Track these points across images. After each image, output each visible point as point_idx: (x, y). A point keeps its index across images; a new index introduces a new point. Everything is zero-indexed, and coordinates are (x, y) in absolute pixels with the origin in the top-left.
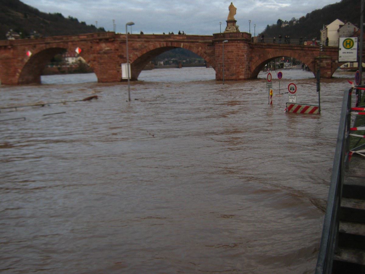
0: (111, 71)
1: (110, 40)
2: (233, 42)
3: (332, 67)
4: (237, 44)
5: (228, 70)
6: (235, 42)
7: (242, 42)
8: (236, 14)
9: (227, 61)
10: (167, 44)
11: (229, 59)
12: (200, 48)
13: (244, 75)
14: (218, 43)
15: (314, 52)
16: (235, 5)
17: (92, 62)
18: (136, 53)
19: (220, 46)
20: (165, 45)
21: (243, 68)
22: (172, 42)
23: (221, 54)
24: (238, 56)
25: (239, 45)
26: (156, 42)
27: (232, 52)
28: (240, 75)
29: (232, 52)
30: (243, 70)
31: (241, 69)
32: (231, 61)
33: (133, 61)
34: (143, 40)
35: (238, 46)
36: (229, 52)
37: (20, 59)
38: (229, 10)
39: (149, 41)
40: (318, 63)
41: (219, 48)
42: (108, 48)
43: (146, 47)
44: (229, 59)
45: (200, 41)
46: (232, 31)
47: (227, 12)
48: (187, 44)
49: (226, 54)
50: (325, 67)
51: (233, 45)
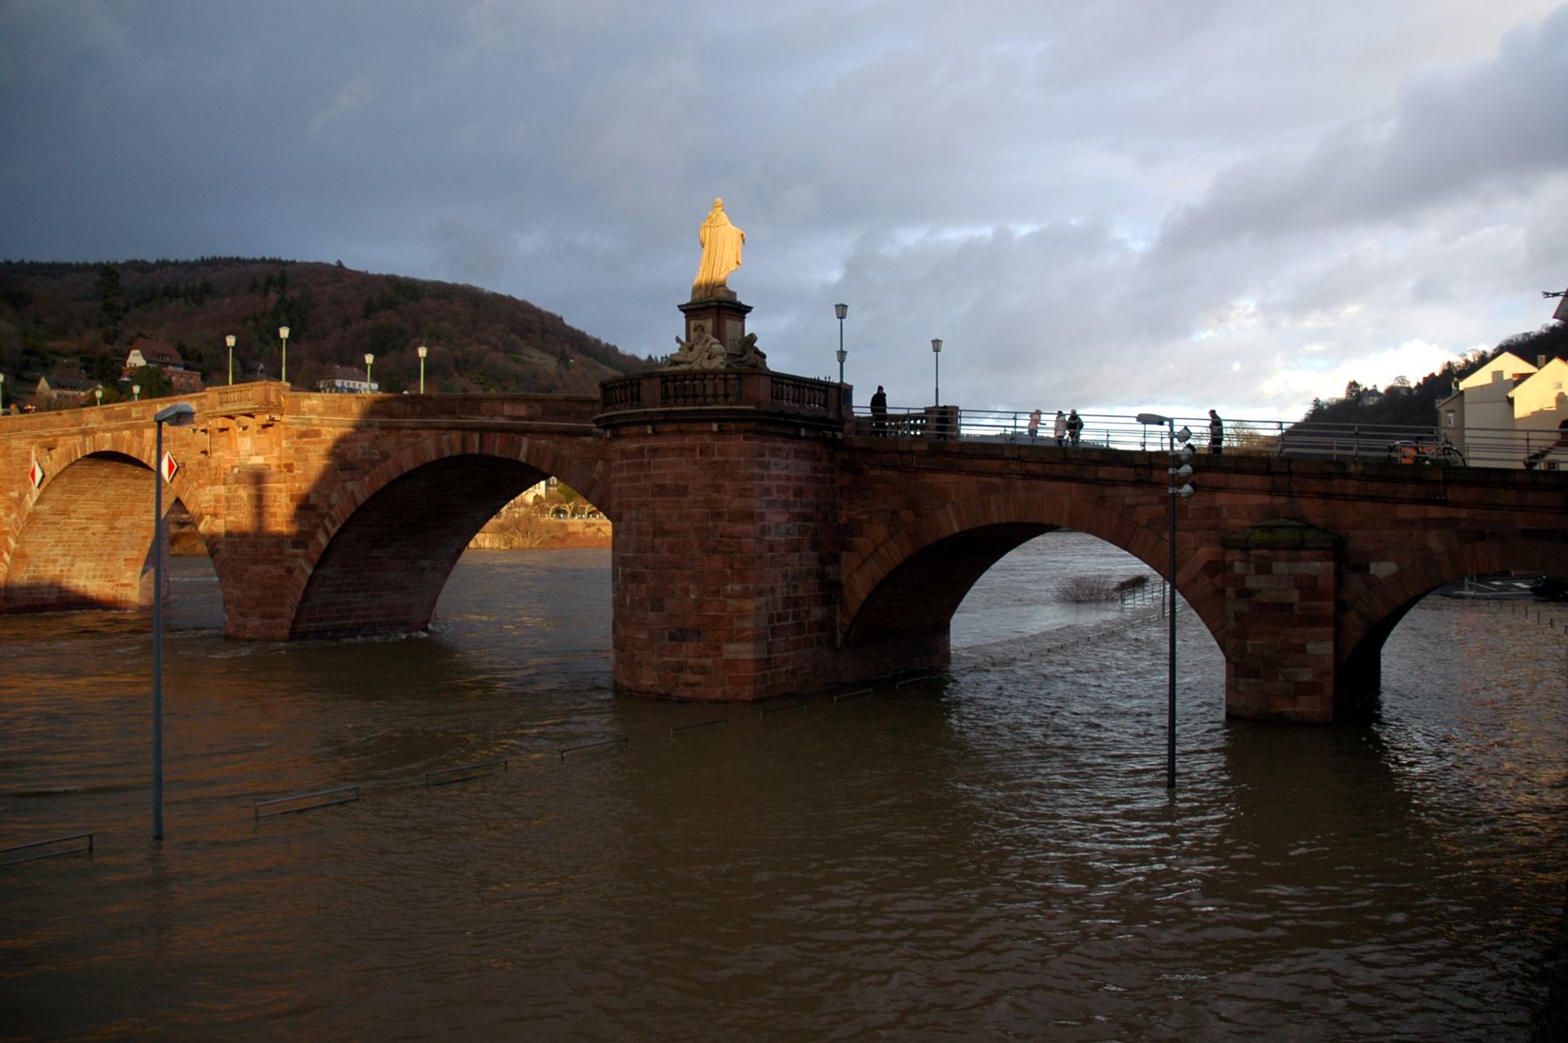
0: (259, 568)
2: (681, 432)
3: (1341, 607)
4: (708, 440)
5: (658, 606)
6: (697, 427)
7: (737, 432)
9: (653, 549)
10: (464, 443)
11: (659, 532)
13: (757, 638)
14: (655, 432)
15: (1222, 499)
18: (350, 485)
20: (458, 451)
21: (745, 595)
22: (483, 430)
24: (718, 515)
25: (722, 452)
26: (424, 433)
27: (681, 491)
28: (731, 640)
29: (681, 491)
30: (749, 605)
31: (732, 603)
32: (671, 550)
33: (339, 526)
35: (717, 458)
36: (661, 490)
39: (399, 429)
40: (1242, 578)
43: (385, 456)
44: (666, 533)
50: (1291, 605)
51: (681, 450)
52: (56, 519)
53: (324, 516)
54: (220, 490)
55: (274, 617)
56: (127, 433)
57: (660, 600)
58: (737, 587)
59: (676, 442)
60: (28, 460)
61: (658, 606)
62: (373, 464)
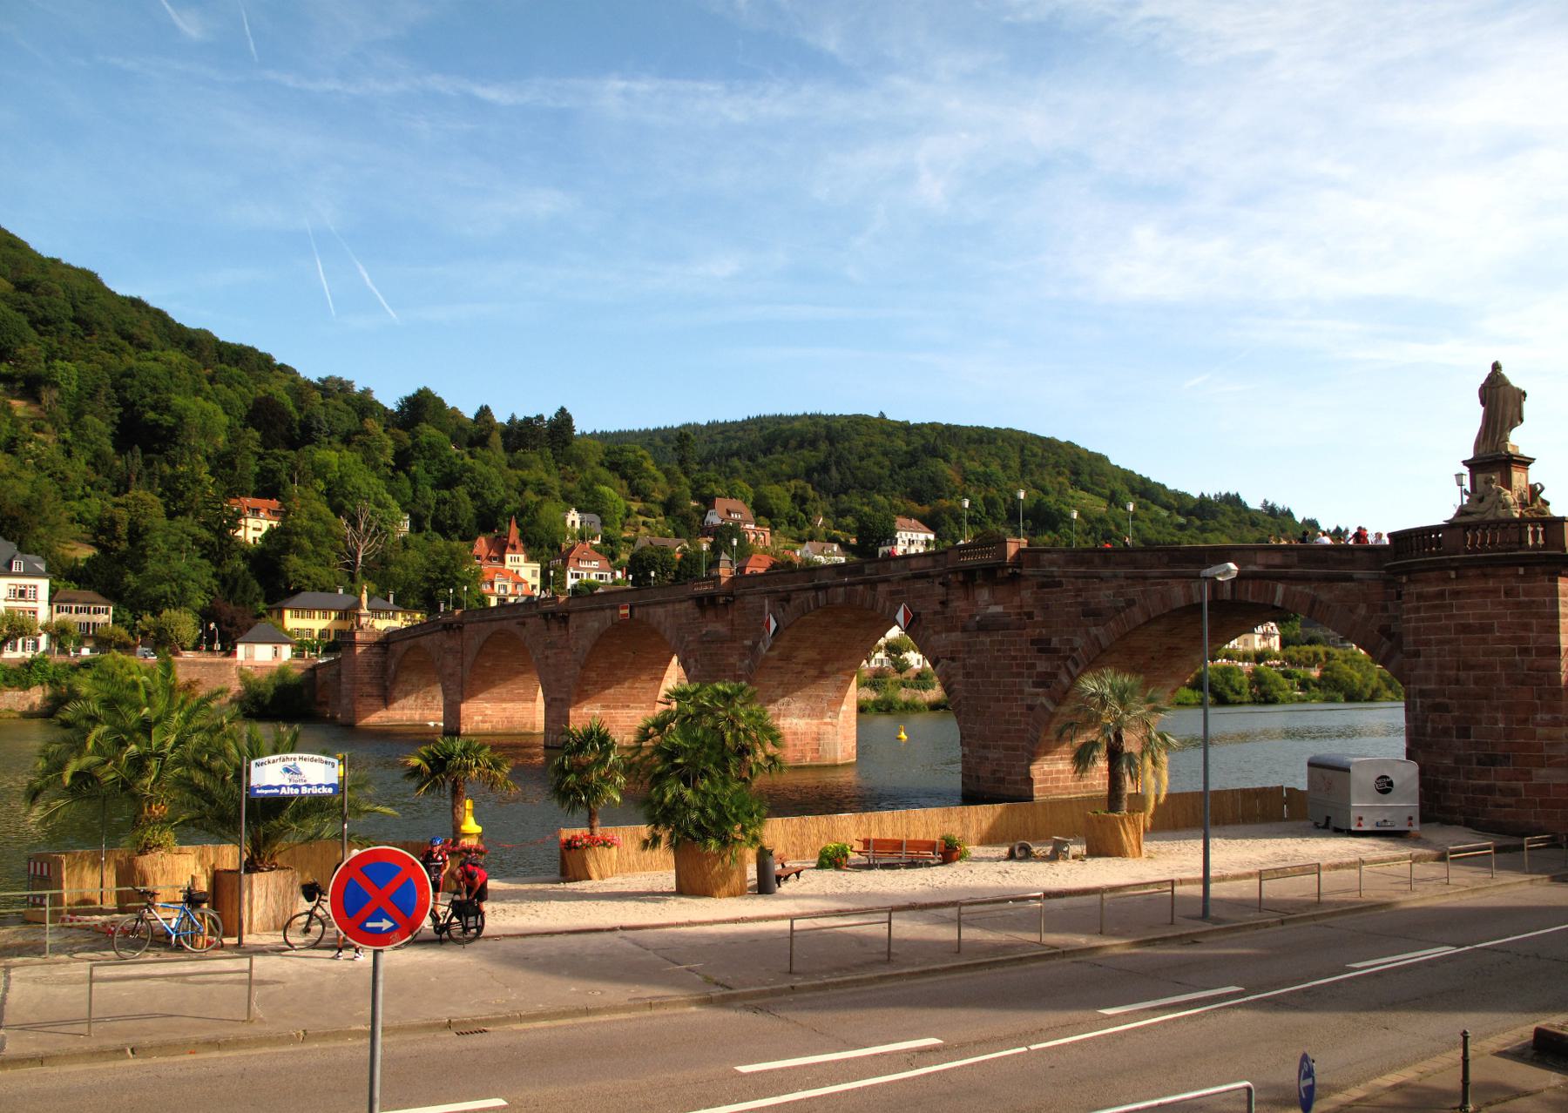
1: (999, 574)
2: (1485, 576)
4: (1513, 583)
6: (1502, 571)
8: (1522, 420)
9: (1457, 681)
12: (1362, 610)
16: (1515, 378)
17: (944, 661)
18: (1093, 630)
19: (1420, 597)
23: (1427, 643)
27: (1486, 629)
29: (1486, 629)
34: (1121, 571)
35: (1522, 598)
36: (1465, 629)
37: (748, 643)
38: (1483, 403)
39: (1145, 578)
41: (1417, 610)
42: (999, 609)
43: (1131, 603)
44: (1472, 668)
45: (1358, 574)
46: (1490, 517)
47: (1474, 415)
48: (1300, 588)
49: (1449, 642)
51: (1486, 593)
52: (780, 664)
53: (1066, 658)
54: (956, 636)
55: (1015, 749)
56: (861, 587)
57: (1467, 730)
58: (1547, 717)
59: (1480, 585)
60: (762, 613)
61: (1464, 733)
62: (1118, 610)
